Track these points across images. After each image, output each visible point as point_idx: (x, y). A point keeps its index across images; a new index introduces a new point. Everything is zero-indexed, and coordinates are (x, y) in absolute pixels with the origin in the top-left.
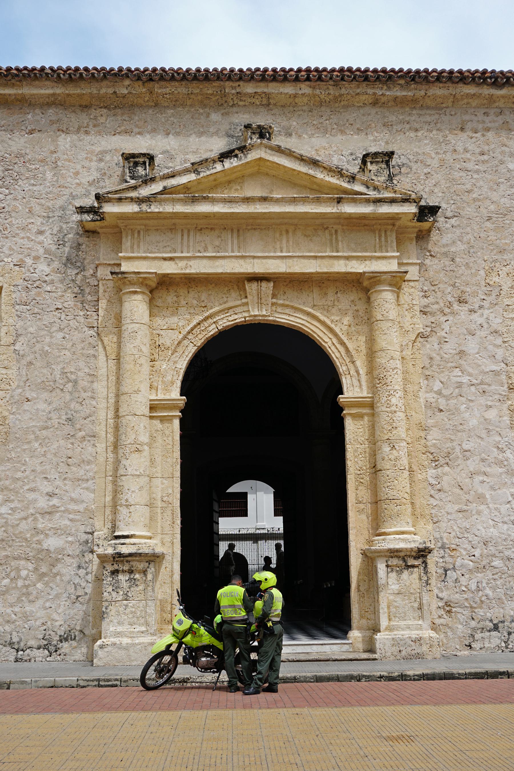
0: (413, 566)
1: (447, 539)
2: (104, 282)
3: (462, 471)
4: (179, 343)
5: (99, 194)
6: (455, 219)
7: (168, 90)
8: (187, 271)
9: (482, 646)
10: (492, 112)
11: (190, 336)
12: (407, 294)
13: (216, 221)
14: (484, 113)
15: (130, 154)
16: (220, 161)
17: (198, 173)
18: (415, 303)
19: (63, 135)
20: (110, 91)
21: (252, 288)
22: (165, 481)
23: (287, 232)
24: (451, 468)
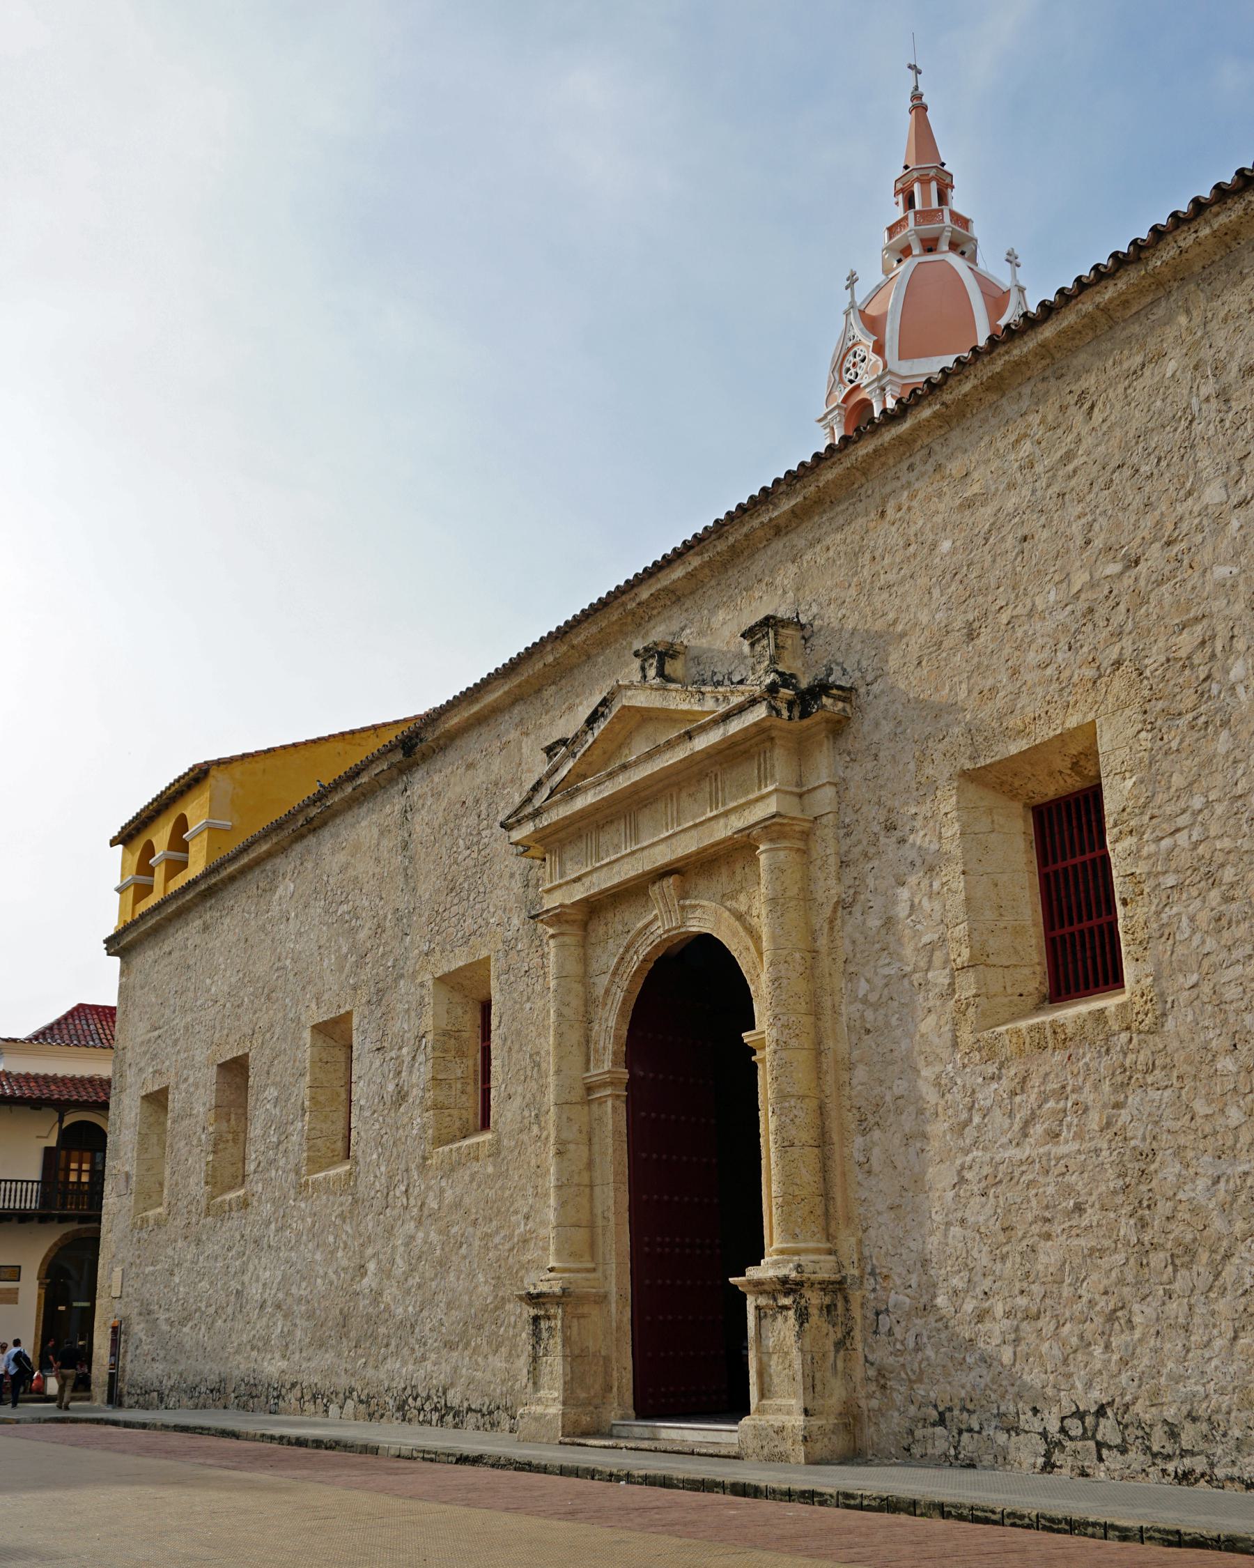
1: (877, 1259)
7: (582, 637)
8: (592, 892)
17: (574, 755)
20: (541, 665)
21: (654, 891)
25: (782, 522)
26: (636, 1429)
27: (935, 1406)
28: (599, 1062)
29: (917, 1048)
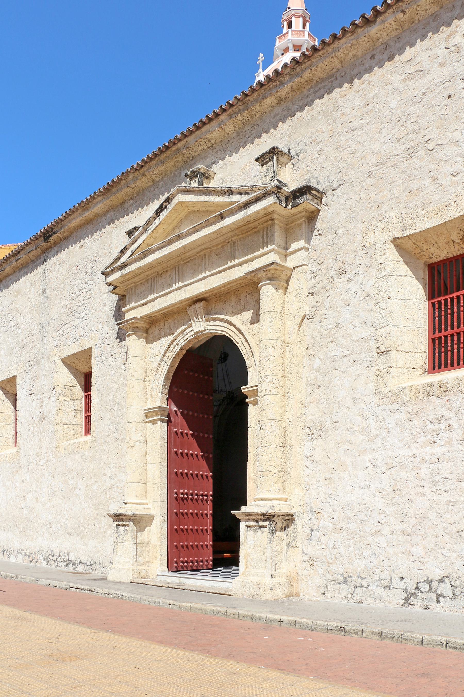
9: (333, 595)
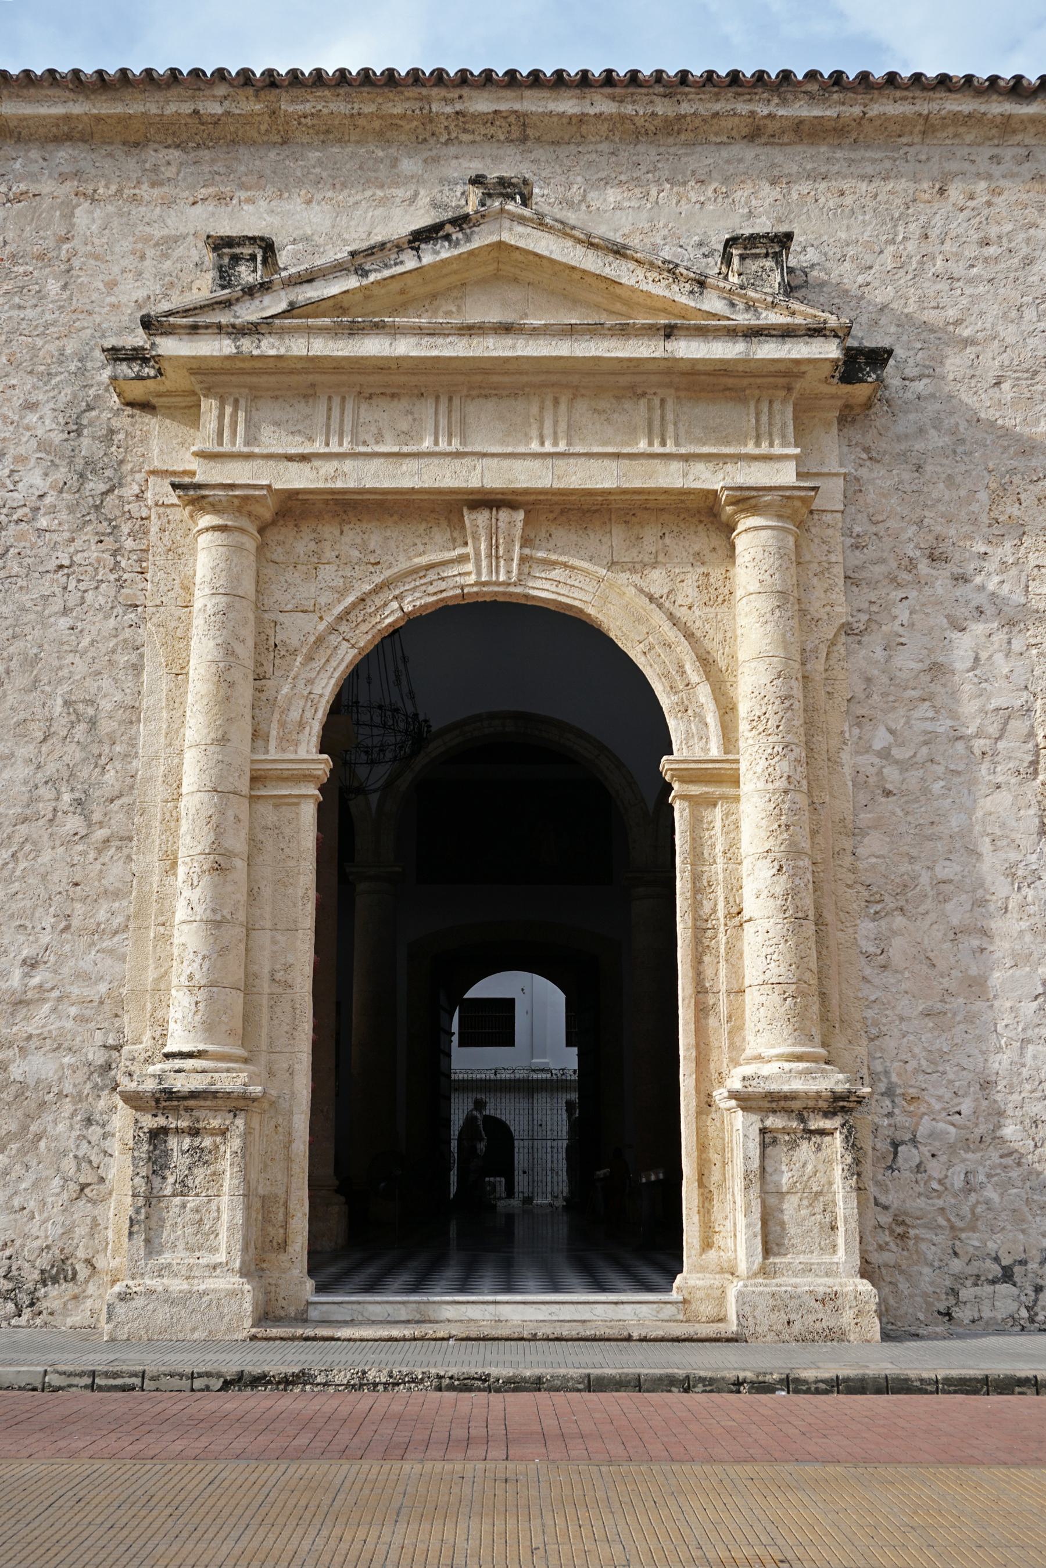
0: (822, 1132)
1: (899, 1075)
2: (161, 510)
3: (935, 926)
4: (320, 640)
5: (148, 315)
6: (925, 381)
7: (308, 108)
8: (339, 485)
10: (1008, 153)
11: (343, 627)
12: (816, 540)
13: (403, 379)
14: (991, 158)
15: (222, 238)
16: (412, 248)
17: (365, 274)
18: (833, 558)
19: (86, 205)
20: (187, 108)
22: (279, 937)
23: (556, 402)
24: (909, 919)
25: (772, 126)
26: (371, 1308)
27: (997, 1259)
28: (287, 740)
29: (977, 828)
